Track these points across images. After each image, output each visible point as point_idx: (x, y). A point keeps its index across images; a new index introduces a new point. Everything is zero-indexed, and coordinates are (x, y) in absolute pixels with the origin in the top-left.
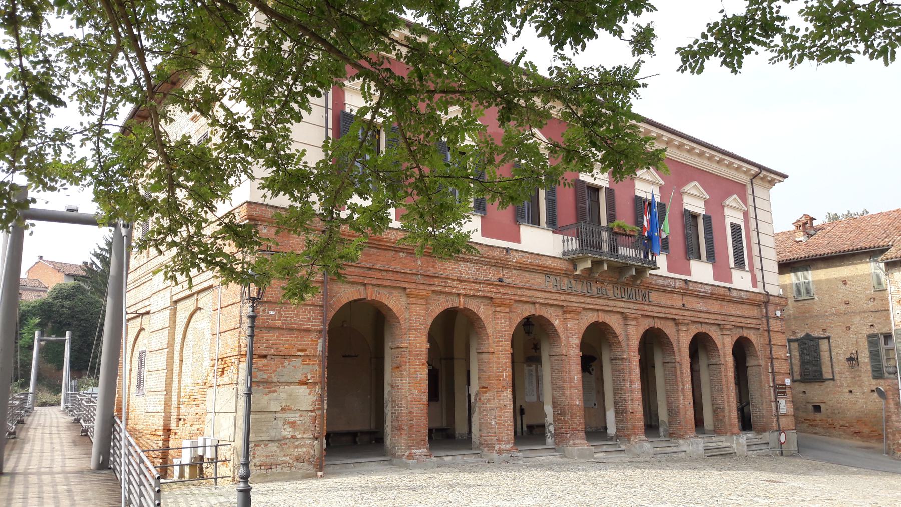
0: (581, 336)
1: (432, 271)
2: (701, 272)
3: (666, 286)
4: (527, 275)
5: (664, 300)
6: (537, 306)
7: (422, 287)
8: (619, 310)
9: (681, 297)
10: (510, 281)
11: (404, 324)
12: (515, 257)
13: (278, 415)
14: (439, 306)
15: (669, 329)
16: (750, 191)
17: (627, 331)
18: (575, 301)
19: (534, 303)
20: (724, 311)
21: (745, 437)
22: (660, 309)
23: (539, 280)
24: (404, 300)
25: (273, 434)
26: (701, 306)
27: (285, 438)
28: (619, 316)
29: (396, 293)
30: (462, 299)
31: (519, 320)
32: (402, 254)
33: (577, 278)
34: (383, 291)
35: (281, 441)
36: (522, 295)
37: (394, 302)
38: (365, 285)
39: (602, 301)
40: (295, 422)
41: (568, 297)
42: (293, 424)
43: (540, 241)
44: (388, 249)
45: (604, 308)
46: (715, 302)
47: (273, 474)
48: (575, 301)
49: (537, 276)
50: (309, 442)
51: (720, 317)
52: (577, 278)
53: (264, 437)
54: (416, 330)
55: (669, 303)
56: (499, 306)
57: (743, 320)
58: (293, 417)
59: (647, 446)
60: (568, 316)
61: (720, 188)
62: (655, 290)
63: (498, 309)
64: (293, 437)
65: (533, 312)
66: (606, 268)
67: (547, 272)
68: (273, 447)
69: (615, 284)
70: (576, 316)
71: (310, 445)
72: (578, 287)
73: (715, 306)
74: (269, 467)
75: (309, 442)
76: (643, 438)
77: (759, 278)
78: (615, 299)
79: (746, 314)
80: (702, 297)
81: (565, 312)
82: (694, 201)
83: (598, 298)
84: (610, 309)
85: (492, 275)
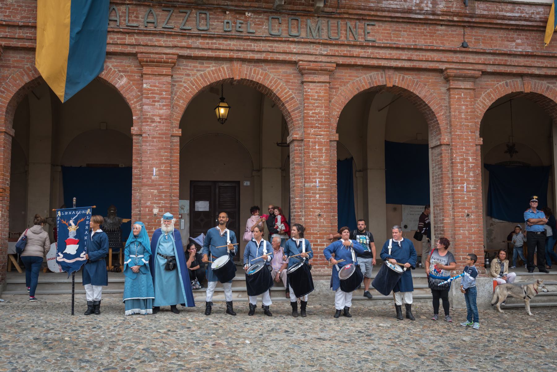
0: (183, 104)
3: (410, 11)
8: (287, 57)
9: (460, 31)
22: (395, 53)
28: (289, 70)
39: (233, 44)
41: (143, 39)
45: (241, 55)
60: (146, 70)
70: (165, 71)
81: (142, 64)
84: (257, 56)
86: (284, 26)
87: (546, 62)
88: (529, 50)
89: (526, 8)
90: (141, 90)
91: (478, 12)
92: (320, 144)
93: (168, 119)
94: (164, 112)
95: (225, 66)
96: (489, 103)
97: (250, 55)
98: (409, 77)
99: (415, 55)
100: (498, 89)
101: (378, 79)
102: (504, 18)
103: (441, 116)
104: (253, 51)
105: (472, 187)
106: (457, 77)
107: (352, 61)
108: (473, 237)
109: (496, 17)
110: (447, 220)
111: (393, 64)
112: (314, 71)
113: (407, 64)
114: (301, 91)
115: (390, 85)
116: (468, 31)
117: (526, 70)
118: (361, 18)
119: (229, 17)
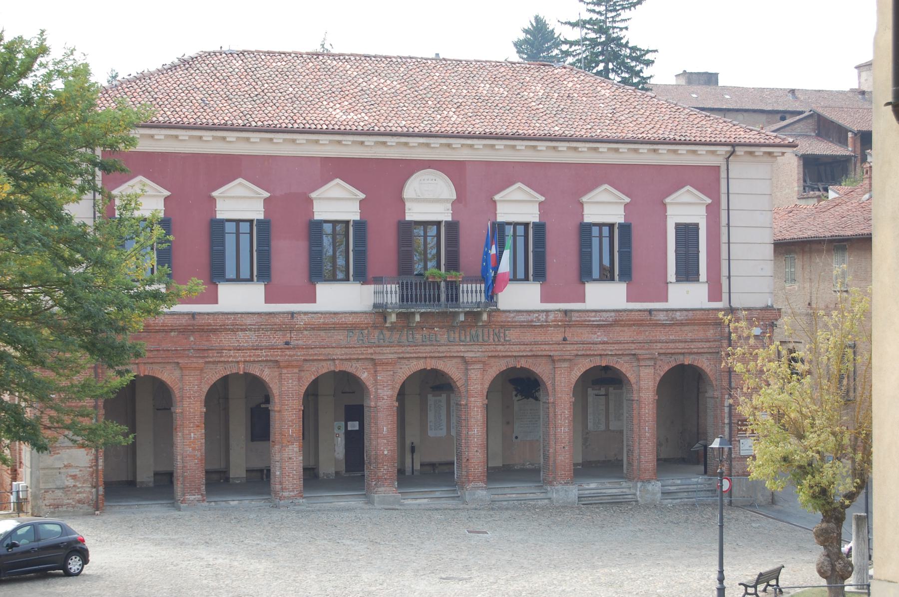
0: (398, 386)
1: (205, 344)
2: (606, 296)
4: (322, 333)
5: (529, 337)
6: (337, 362)
7: (195, 360)
8: (459, 354)
10: (300, 342)
11: (177, 393)
12: (301, 321)
13: (62, 471)
14: (214, 375)
15: (541, 369)
16: (723, 175)
17: (466, 374)
18: (388, 354)
19: (334, 360)
20: (641, 338)
21: (659, 484)
22: (522, 347)
23: (340, 337)
24: (177, 373)
25: (58, 483)
26: (599, 336)
27: (67, 487)
28: (459, 360)
29: (169, 367)
30: (242, 366)
31: (313, 378)
32: (173, 334)
33: (392, 328)
34: (155, 367)
35: (65, 489)
36: (316, 354)
37: (167, 375)
38: (137, 364)
39: (428, 349)
40: (75, 476)
41: (378, 350)
42: (74, 477)
43: (342, 298)
44: (158, 331)
46: (626, 329)
47: (60, 512)
48: (388, 354)
49: (336, 332)
50: (88, 489)
51: (633, 346)
52: (392, 328)
53: (51, 486)
54: (189, 398)
55: (539, 339)
56: (287, 367)
57: (681, 345)
58: (75, 472)
59: (482, 494)
60: (379, 368)
61: (649, 185)
62: (515, 327)
63: (285, 371)
64: (74, 486)
65: (332, 368)
66: (418, 318)
67: (351, 328)
68: (59, 493)
69: (452, 328)
70: (389, 368)
71: (86, 491)
72: (396, 336)
73: (626, 334)
74: (57, 506)
75: (88, 489)
76: (481, 484)
77: (725, 288)
78: (450, 343)
79: (690, 336)
80: (599, 326)
82: (604, 207)
83: (423, 345)
84: (441, 355)
85: (278, 340)
86: (457, 335)
87: (616, 347)
88: (606, 339)
89: (604, 314)
90: (376, 380)
91: (573, 319)
92: (477, 407)
93: (392, 396)
94: (389, 393)
95: (422, 361)
96: (579, 374)
97: (437, 355)
98: (530, 360)
99: (534, 348)
100: (584, 365)
101: (512, 363)
102: (590, 321)
103: (549, 384)
104: (439, 352)
105: (567, 430)
106: (559, 360)
107: (497, 354)
108: (567, 461)
109: (585, 321)
110: (551, 450)
111: (521, 354)
112: (475, 362)
113: (529, 354)
114: (466, 374)
115: (518, 366)
116: (567, 329)
117: (603, 352)
118: (502, 327)
119: (425, 331)
